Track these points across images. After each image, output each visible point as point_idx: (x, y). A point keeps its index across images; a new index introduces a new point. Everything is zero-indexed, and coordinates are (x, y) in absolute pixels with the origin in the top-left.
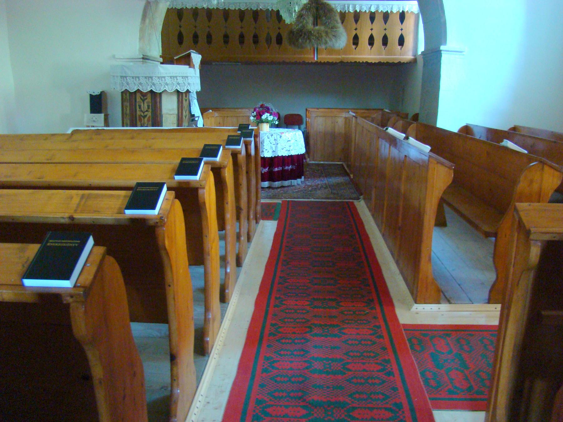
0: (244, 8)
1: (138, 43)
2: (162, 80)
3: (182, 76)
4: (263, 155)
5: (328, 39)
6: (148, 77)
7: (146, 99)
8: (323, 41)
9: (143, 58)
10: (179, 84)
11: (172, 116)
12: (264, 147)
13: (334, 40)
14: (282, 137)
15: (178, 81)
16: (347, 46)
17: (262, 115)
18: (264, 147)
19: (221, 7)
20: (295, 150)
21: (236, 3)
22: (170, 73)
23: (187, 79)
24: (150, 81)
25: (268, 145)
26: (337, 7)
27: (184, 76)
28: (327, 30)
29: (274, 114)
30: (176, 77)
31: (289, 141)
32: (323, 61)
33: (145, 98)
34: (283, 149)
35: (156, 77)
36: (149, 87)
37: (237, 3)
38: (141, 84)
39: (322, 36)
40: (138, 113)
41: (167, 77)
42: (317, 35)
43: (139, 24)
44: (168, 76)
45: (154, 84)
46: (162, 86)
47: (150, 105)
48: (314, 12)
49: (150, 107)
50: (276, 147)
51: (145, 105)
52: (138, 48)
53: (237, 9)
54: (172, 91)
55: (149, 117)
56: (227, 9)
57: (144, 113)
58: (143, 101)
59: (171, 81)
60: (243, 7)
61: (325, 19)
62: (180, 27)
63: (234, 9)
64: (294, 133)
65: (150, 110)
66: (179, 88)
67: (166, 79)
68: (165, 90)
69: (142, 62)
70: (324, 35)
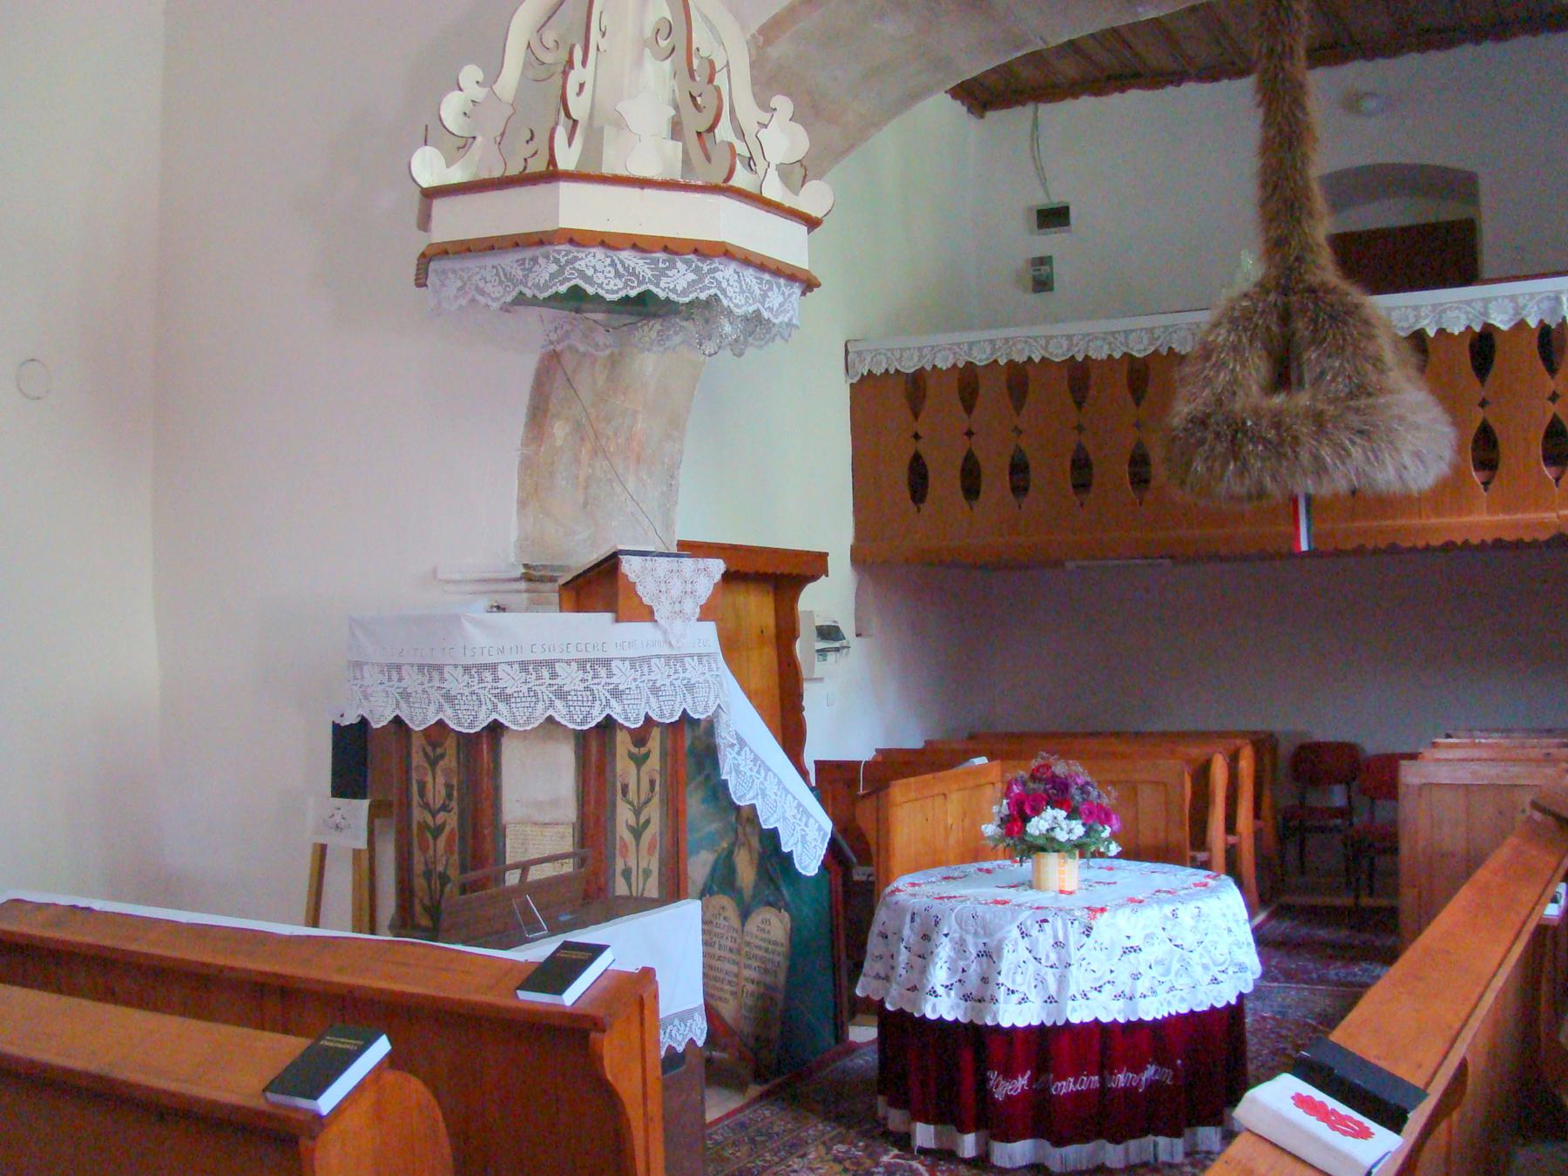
0: (1145, 350)
1: (514, 519)
2: (481, 681)
3: (576, 661)
4: (995, 1017)
5: (1326, 453)
6: (430, 666)
7: (442, 756)
8: (1305, 457)
9: (527, 578)
10: (561, 694)
11: (549, 831)
12: (1001, 979)
13: (1356, 452)
14: (1093, 933)
15: (558, 681)
16: (1457, 475)
18: (1001, 979)
19: (1057, 356)
20: (1172, 989)
21: (1113, 333)
25: (1020, 970)
27: (586, 661)
28: (1320, 406)
29: (1091, 813)
30: (550, 664)
31: (1134, 949)
33: (439, 751)
34: (1099, 989)
35: (456, 666)
36: (432, 708)
37: (1119, 332)
38: (405, 695)
39: (1296, 439)
40: (418, 815)
41: (507, 668)
42: (1271, 434)
44: (510, 664)
45: (450, 698)
46: (484, 707)
47: (455, 782)
48: (1268, 328)
49: (455, 793)
50: (1062, 981)
51: (437, 780)
52: (514, 536)
53: (1117, 355)
54: (529, 728)
55: (453, 830)
56: (1080, 358)
58: (433, 763)
59: (526, 682)
60: (1142, 347)
63: (1104, 357)
64: (1168, 909)
65: (454, 804)
66: (564, 711)
67: (500, 674)
68: (495, 720)
69: (527, 591)
70: (1305, 430)
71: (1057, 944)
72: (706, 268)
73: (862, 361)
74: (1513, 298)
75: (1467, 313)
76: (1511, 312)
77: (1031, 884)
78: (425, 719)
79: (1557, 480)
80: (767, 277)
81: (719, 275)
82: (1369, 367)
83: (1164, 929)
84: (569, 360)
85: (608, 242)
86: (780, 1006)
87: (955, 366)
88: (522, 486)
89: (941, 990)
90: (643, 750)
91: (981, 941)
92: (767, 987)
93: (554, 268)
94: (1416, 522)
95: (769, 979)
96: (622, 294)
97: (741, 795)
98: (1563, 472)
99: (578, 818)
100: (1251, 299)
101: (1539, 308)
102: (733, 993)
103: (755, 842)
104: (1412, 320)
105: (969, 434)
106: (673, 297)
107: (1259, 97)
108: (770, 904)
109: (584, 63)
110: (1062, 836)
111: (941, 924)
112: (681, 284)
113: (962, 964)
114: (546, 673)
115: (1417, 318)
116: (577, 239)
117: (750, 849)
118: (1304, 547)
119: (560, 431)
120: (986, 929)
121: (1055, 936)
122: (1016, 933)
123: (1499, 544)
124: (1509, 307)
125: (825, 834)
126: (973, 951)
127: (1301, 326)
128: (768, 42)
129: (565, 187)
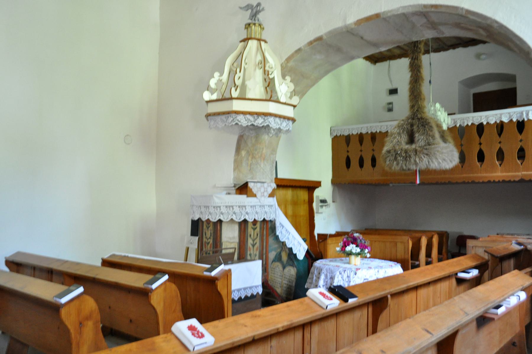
7: (210, 227)
8: (412, 160)
10: (235, 213)
17: (346, 247)
22: (226, 203)
23: (244, 208)
24: (208, 210)
26: (512, 116)
30: (232, 207)
32: (497, 180)
33: (209, 225)
36: (207, 216)
40: (204, 240)
43: (233, 156)
45: (210, 213)
52: (232, 177)
57: (208, 240)
58: (208, 228)
61: (418, 136)
62: (348, 152)
65: (212, 237)
67: (221, 208)
71: (348, 277)
72: (266, 118)
73: (334, 132)
74: (509, 113)
75: (495, 118)
76: (508, 117)
77: (349, 263)
78: (205, 218)
79: (521, 164)
80: (282, 119)
81: (269, 120)
82: (430, 138)
83: (375, 275)
84: (245, 137)
85: (244, 113)
86: (293, 291)
87: (357, 133)
88: (234, 166)
89: (321, 286)
90: (255, 227)
91: (331, 275)
92: (290, 286)
93: (232, 119)
94: (479, 175)
95: (289, 284)
96: (247, 124)
97: (282, 239)
98: (482, 164)
99: (239, 241)
100: (404, 121)
101: (517, 116)
102: (281, 287)
103: (287, 250)
104: (479, 120)
105: (361, 151)
106: (258, 125)
107: (410, 70)
108: (290, 265)
109: (240, 72)
110: (354, 251)
111: (322, 270)
112: (260, 122)
113: (326, 280)
114: (231, 208)
115: (481, 119)
116: (237, 113)
117: (286, 251)
118: (418, 182)
119: (243, 153)
120: (332, 272)
121: (348, 274)
122: (338, 273)
123: (504, 181)
124: (508, 116)
125: (305, 250)
126: (329, 277)
127: (415, 128)
128: (288, 62)
129: (234, 102)
